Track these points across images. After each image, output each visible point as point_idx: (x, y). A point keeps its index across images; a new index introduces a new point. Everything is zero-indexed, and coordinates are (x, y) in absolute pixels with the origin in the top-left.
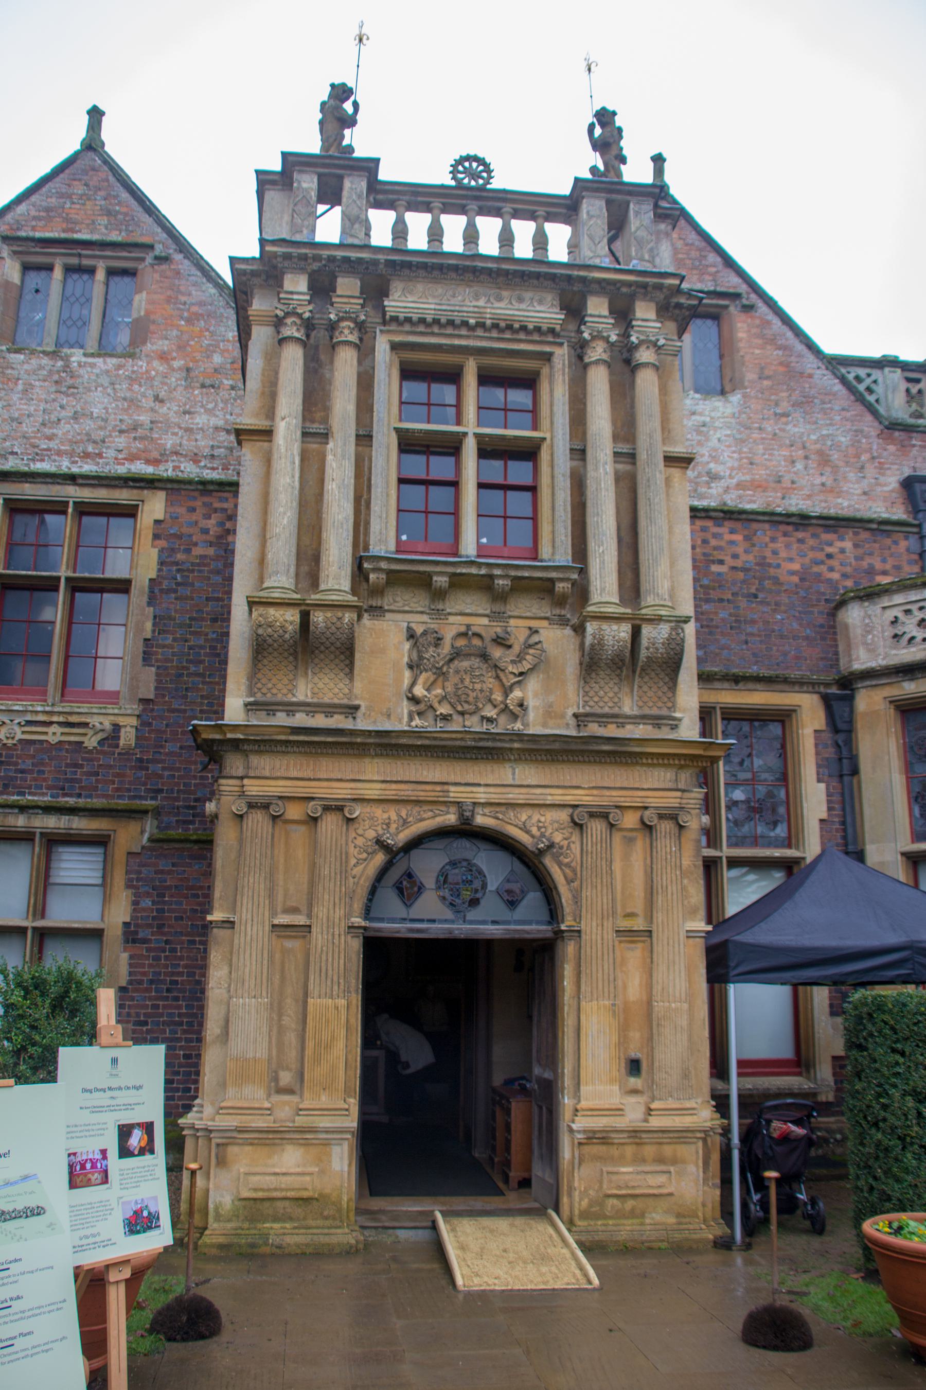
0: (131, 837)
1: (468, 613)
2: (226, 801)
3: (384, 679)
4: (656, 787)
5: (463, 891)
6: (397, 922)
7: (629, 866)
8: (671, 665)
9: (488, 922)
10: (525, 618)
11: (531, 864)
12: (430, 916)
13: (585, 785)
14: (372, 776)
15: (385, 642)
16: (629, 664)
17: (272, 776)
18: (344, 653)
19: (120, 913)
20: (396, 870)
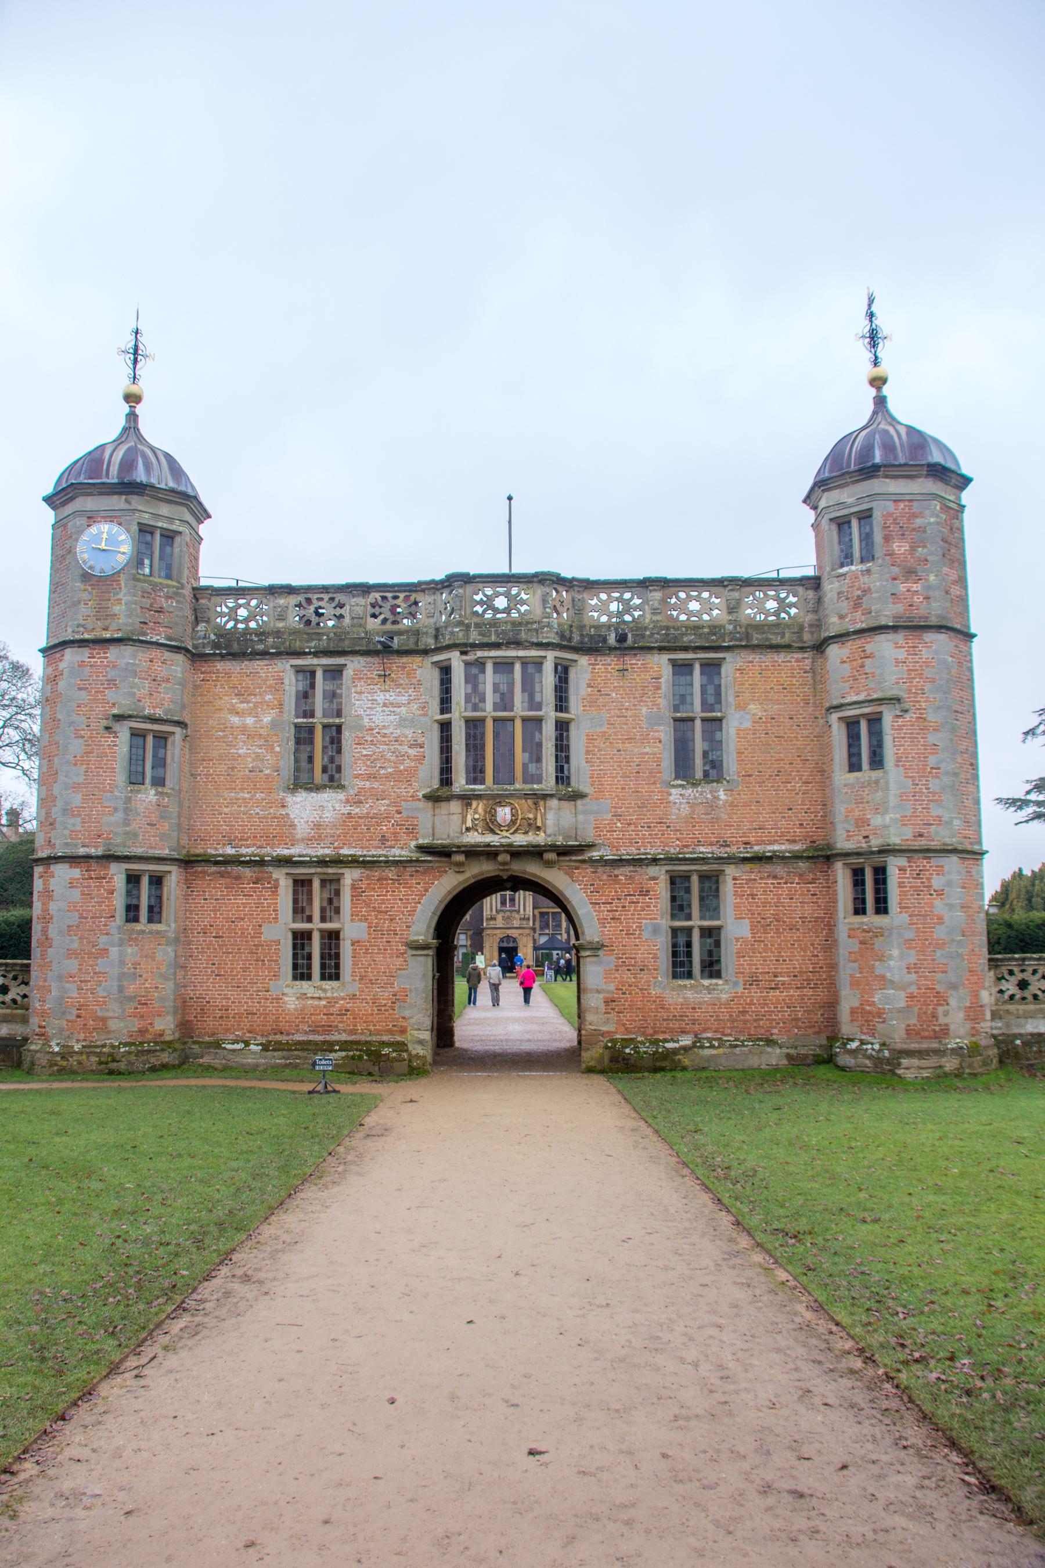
0: (470, 933)
1: (508, 914)
2: (484, 934)
3: (499, 922)
4: (527, 931)
5: (508, 942)
6: (502, 945)
7: (525, 939)
8: (528, 919)
9: (511, 945)
10: (514, 914)
11: (515, 940)
12: (505, 945)
13: (520, 931)
14: (498, 931)
15: (499, 917)
16: (524, 919)
17: (488, 932)
18: (495, 919)
19: (469, 943)
20: (502, 940)
